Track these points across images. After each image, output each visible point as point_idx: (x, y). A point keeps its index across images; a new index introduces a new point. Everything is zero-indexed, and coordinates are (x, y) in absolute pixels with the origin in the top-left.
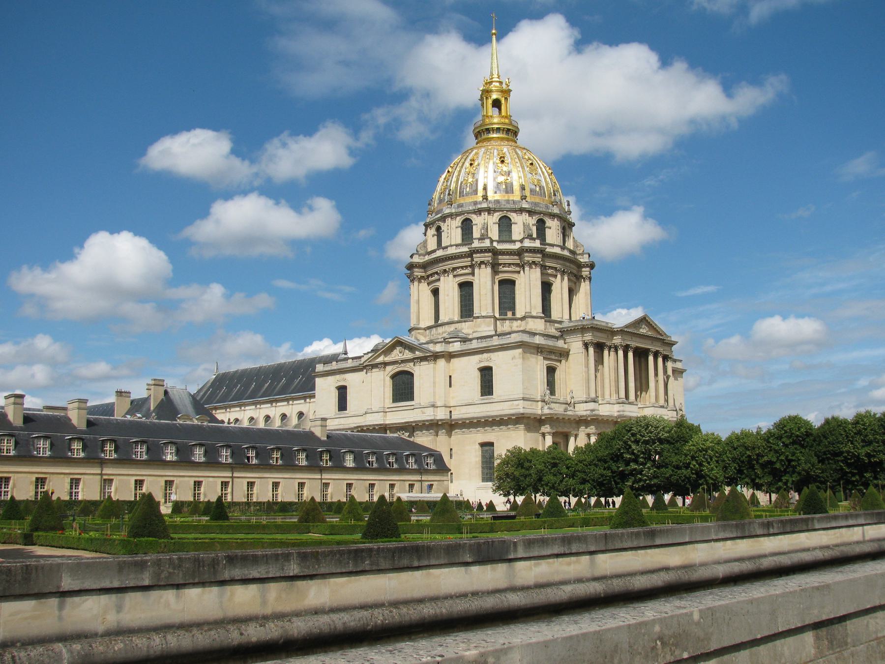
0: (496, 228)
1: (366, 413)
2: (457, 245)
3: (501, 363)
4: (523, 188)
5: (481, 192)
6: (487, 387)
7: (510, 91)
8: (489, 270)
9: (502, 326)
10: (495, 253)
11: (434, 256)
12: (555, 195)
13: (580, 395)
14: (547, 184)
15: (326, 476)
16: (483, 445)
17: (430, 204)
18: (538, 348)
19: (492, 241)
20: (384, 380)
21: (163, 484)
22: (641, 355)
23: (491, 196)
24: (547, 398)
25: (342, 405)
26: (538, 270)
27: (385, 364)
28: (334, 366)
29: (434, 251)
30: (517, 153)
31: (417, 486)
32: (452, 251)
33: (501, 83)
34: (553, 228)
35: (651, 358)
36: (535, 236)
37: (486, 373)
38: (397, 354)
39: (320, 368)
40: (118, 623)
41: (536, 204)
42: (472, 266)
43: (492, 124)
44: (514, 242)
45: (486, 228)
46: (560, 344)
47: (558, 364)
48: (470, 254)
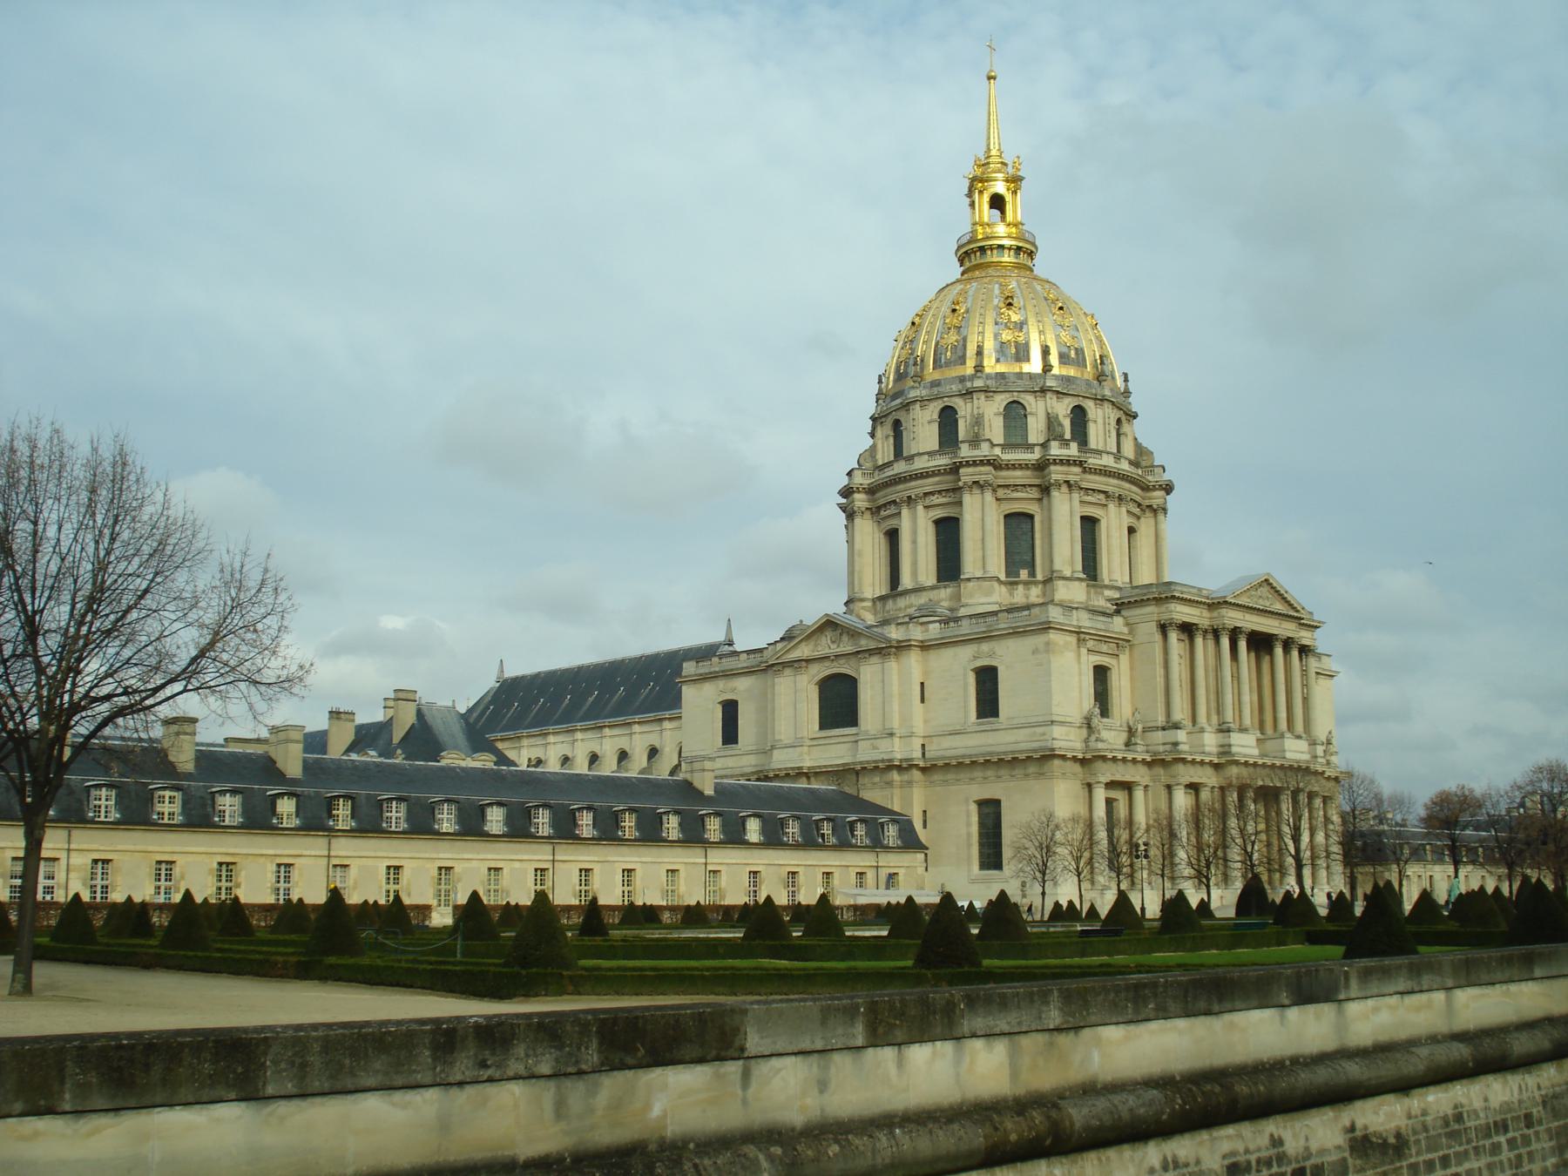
0: (998, 423)
1: (773, 748)
2: (928, 453)
4: (1046, 352)
5: (971, 363)
6: (988, 704)
7: (1020, 179)
8: (989, 496)
9: (1011, 594)
10: (996, 464)
11: (889, 473)
12: (1102, 363)
16: (982, 804)
19: (993, 445)
21: (436, 872)
23: (991, 365)
24: (1096, 721)
25: (730, 734)
26: (1076, 496)
28: (715, 665)
29: (888, 465)
31: (870, 875)
32: (921, 464)
33: (1004, 164)
35: (1279, 651)
36: (1068, 436)
37: (987, 680)
38: (826, 646)
39: (689, 668)
40: (822, 1110)
41: (1068, 380)
42: (957, 490)
43: (987, 238)
45: (978, 421)
48: (955, 469)
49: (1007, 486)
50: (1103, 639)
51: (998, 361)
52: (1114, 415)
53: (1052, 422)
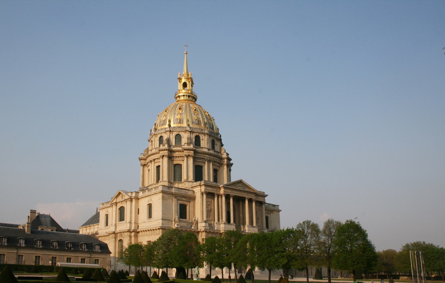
0: (174, 139)
5: (168, 123)
13: (200, 220)
14: (203, 119)
17: (151, 131)
20: (116, 211)
22: (239, 201)
23: (172, 125)
27: (116, 203)
30: (189, 106)
32: (154, 151)
35: (247, 202)
38: (119, 199)
44: (181, 146)
46: (190, 193)
47: (187, 203)
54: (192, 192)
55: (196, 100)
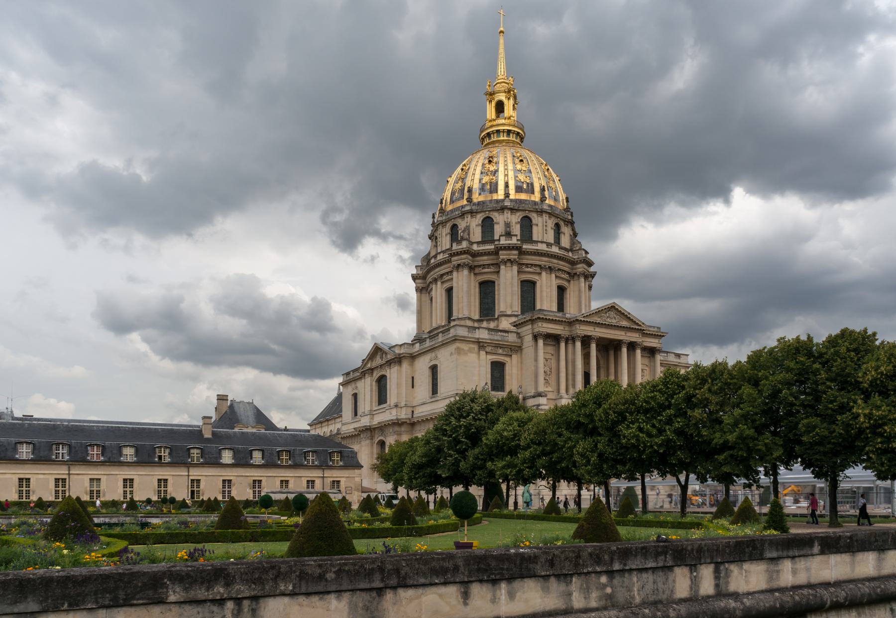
3: (445, 358)
4: (507, 185)
8: (466, 272)
15: (195, 473)
18: (479, 342)
19: (472, 243)
23: (475, 200)
26: (515, 268)
31: (318, 483)
32: (440, 257)
34: (540, 225)
41: (521, 201)
42: (451, 272)
43: (492, 126)
44: (492, 241)
45: (467, 229)
46: (512, 338)
47: (507, 359)
49: (480, 266)
50: (497, 346)
51: (480, 194)
52: (551, 223)
53: (508, 225)
54: (515, 335)
55: (522, 139)
